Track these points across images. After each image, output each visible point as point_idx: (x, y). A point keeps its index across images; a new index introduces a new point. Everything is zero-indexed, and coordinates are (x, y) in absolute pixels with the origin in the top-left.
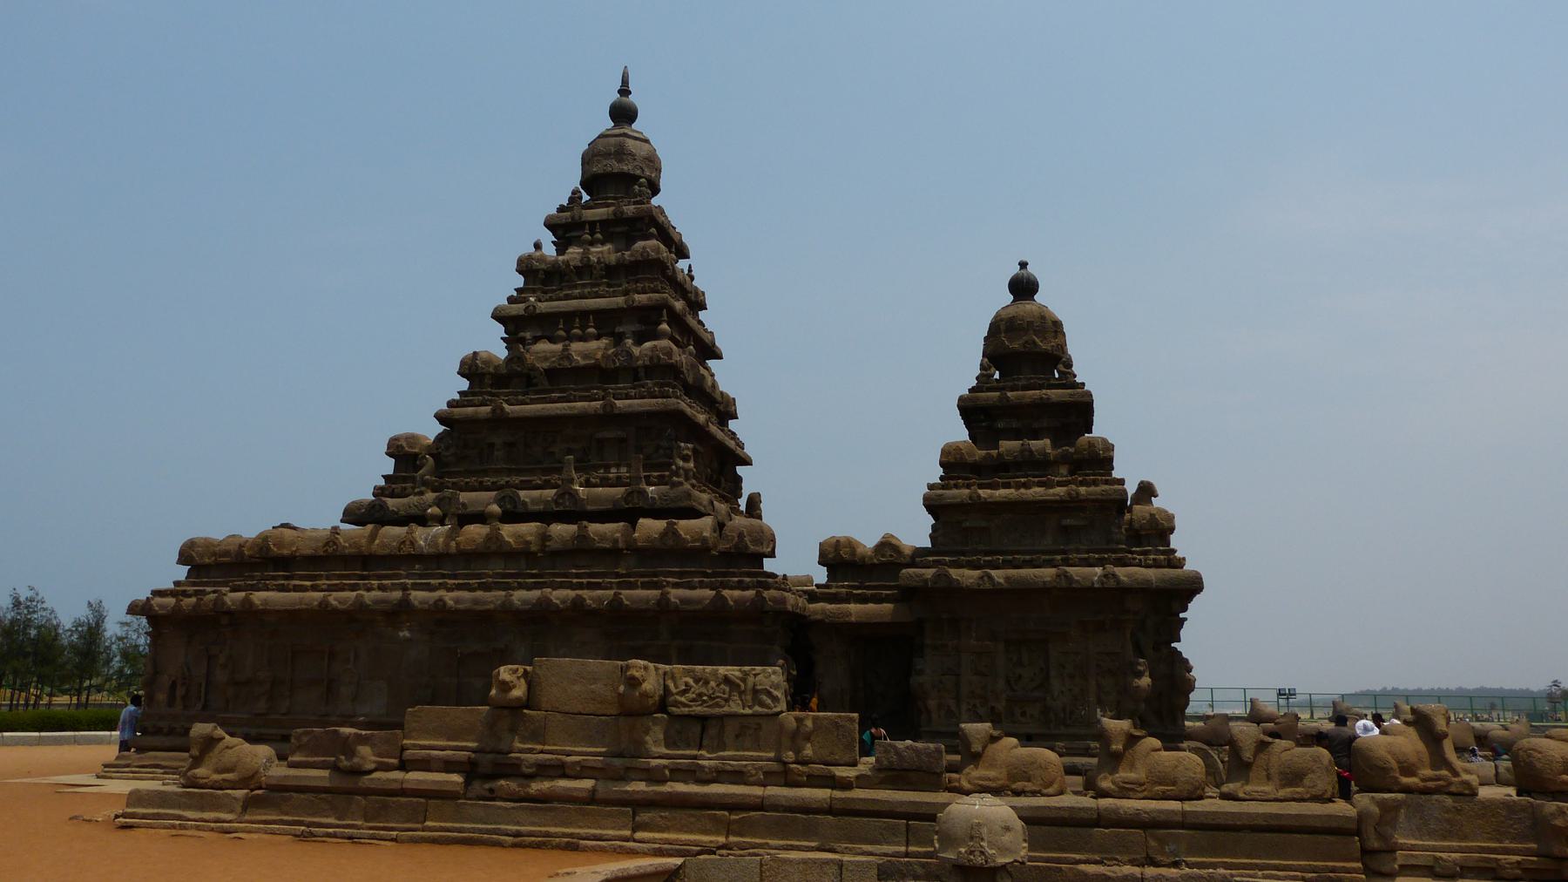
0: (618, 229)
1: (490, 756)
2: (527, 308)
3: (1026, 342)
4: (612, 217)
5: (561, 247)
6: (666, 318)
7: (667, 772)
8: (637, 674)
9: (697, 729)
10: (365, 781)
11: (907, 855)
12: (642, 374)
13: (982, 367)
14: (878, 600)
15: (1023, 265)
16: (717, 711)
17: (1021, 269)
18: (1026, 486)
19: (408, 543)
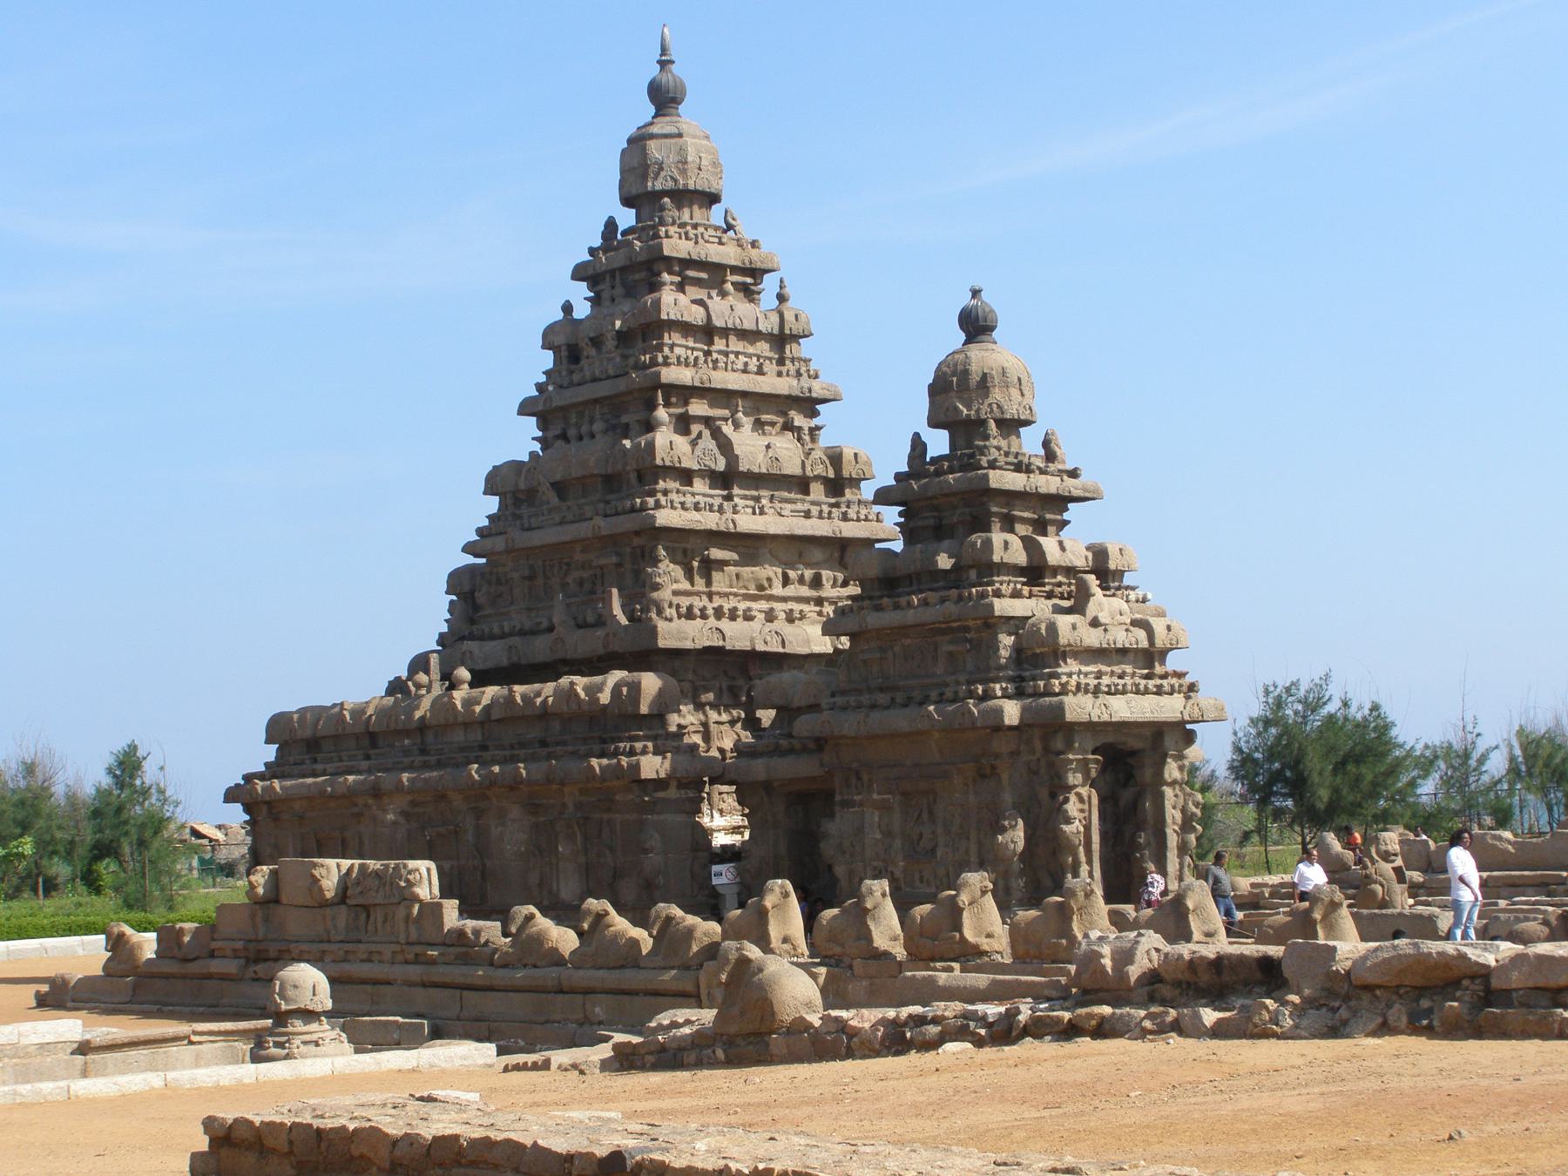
0: (637, 276)
1: (254, 944)
2: (545, 401)
3: (948, 409)
4: (628, 263)
5: (596, 301)
6: (661, 402)
7: (341, 952)
8: (316, 873)
9: (363, 916)
10: (192, 968)
11: (458, 1019)
12: (633, 477)
13: (918, 445)
14: (804, 749)
15: (976, 293)
16: (370, 901)
17: (974, 296)
19: (393, 718)
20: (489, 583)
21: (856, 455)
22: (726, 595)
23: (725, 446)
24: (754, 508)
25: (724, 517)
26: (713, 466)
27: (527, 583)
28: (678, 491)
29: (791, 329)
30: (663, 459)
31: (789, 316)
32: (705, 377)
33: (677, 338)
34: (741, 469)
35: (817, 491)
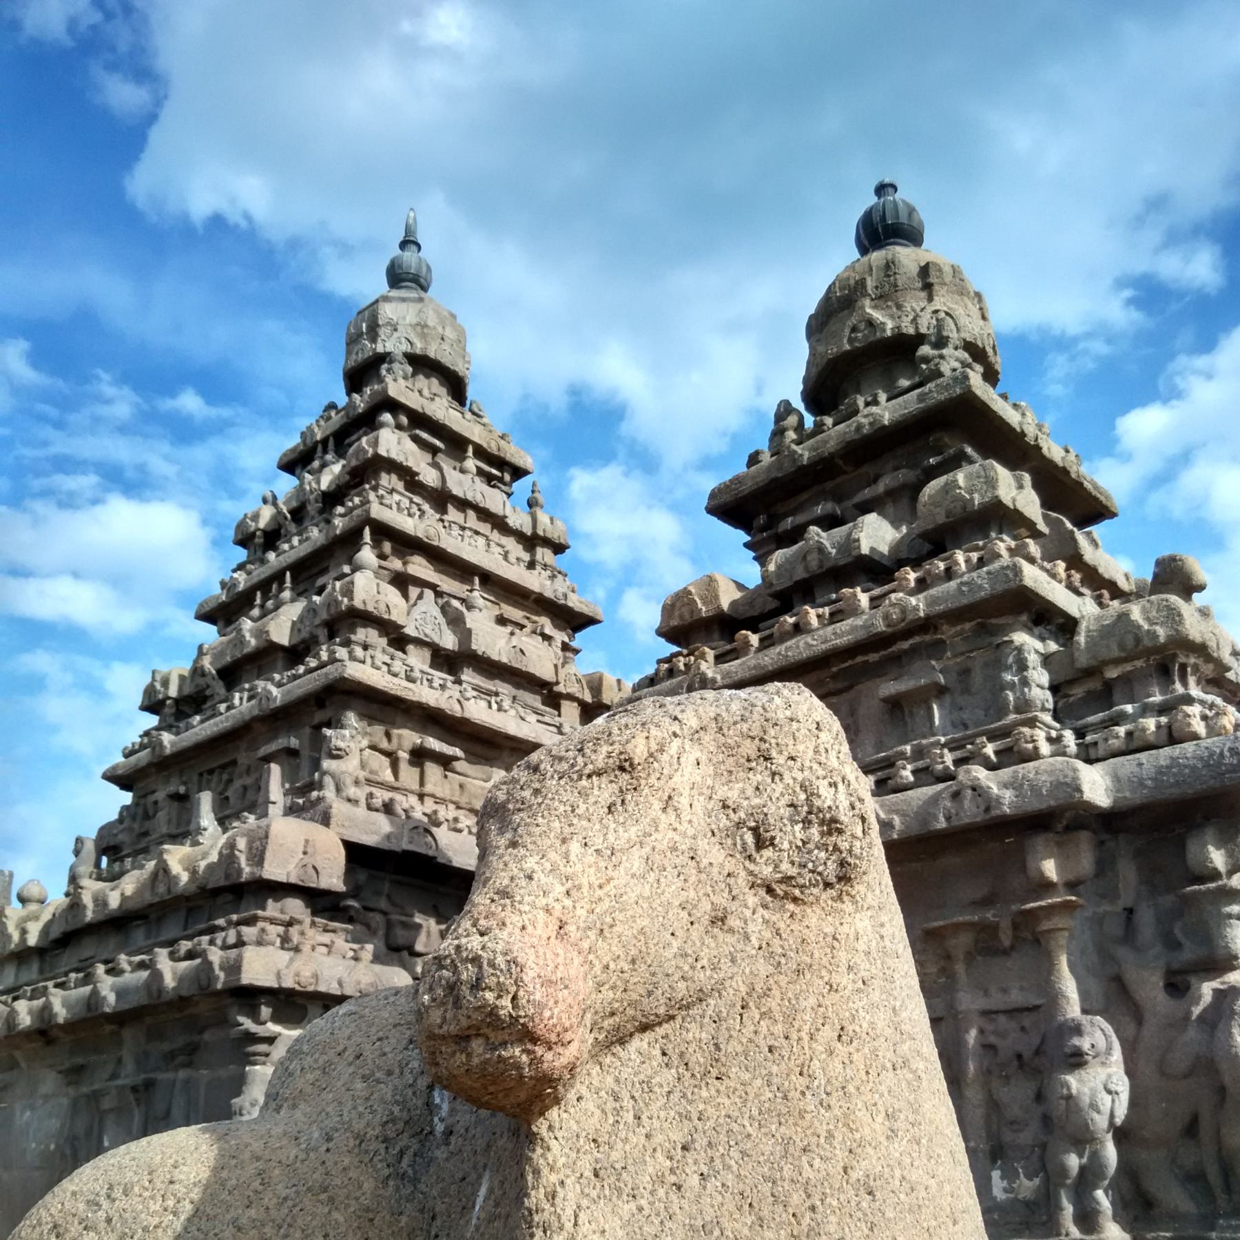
6: (369, 541)
12: (322, 634)
18: (798, 629)
20: (134, 818)
21: (619, 681)
22: (439, 801)
23: (455, 621)
24: (489, 703)
25: (447, 693)
26: (436, 640)
27: (176, 804)
28: (384, 651)
29: (544, 531)
30: (364, 602)
31: (543, 518)
32: (432, 532)
33: (400, 486)
34: (474, 647)
35: (570, 712)
